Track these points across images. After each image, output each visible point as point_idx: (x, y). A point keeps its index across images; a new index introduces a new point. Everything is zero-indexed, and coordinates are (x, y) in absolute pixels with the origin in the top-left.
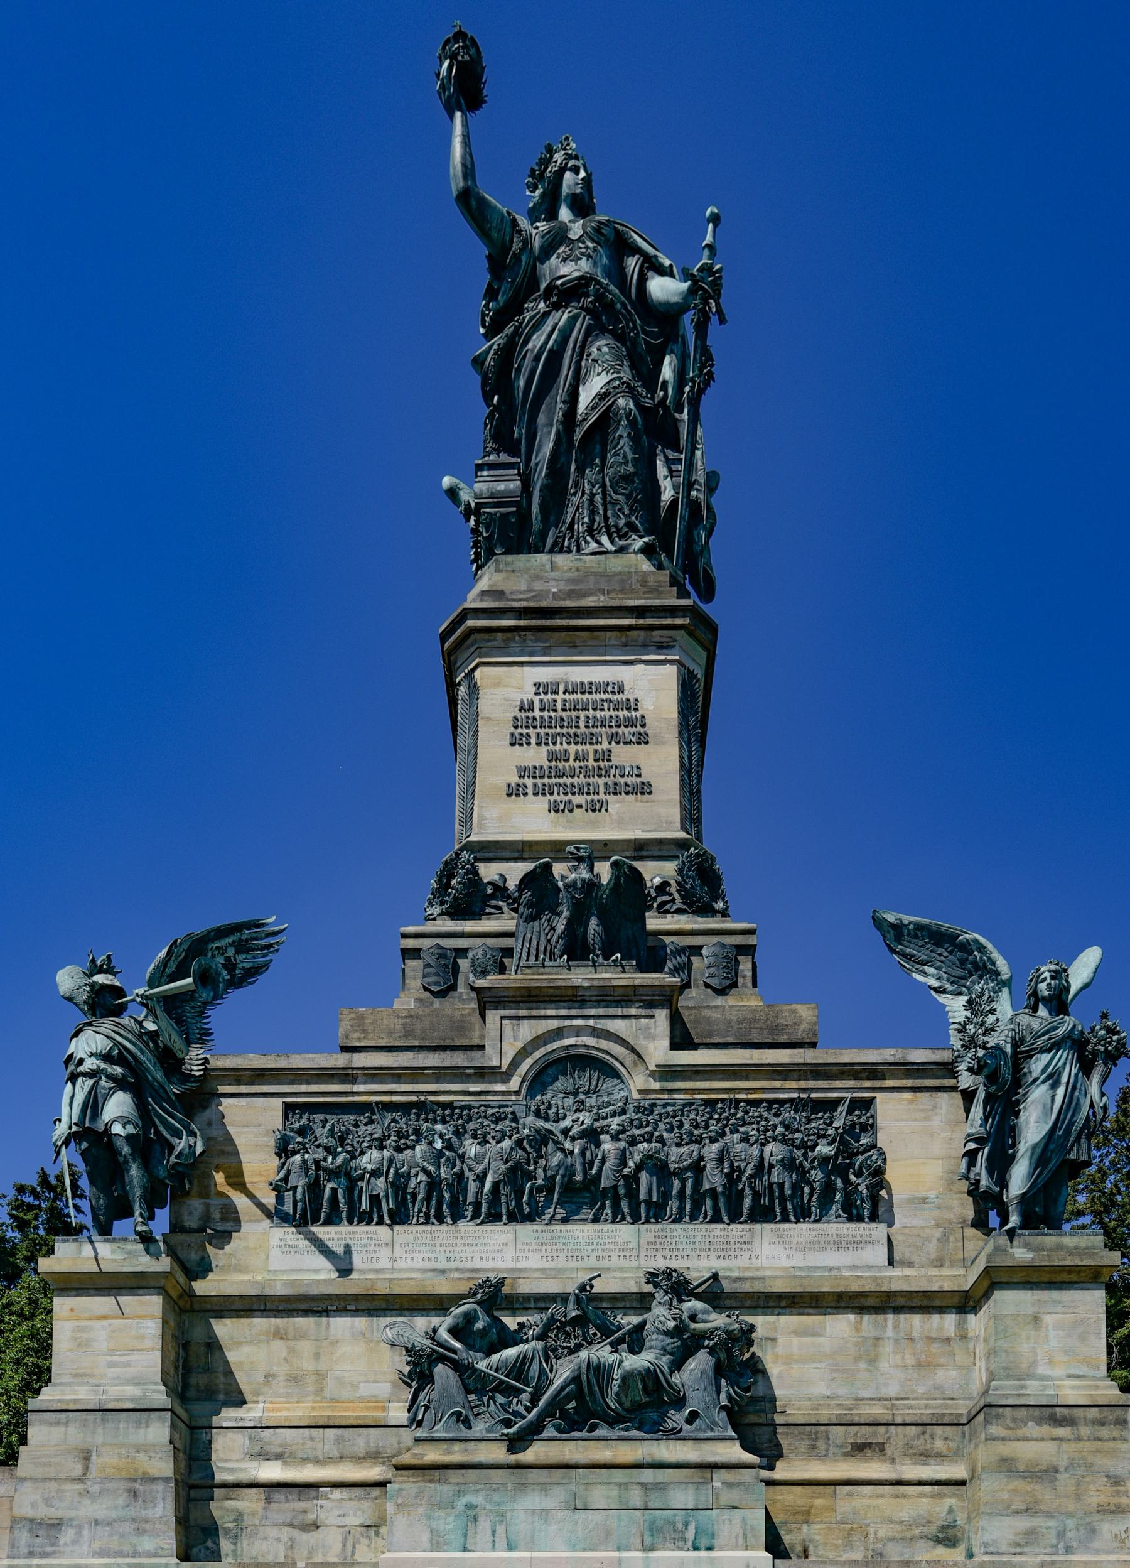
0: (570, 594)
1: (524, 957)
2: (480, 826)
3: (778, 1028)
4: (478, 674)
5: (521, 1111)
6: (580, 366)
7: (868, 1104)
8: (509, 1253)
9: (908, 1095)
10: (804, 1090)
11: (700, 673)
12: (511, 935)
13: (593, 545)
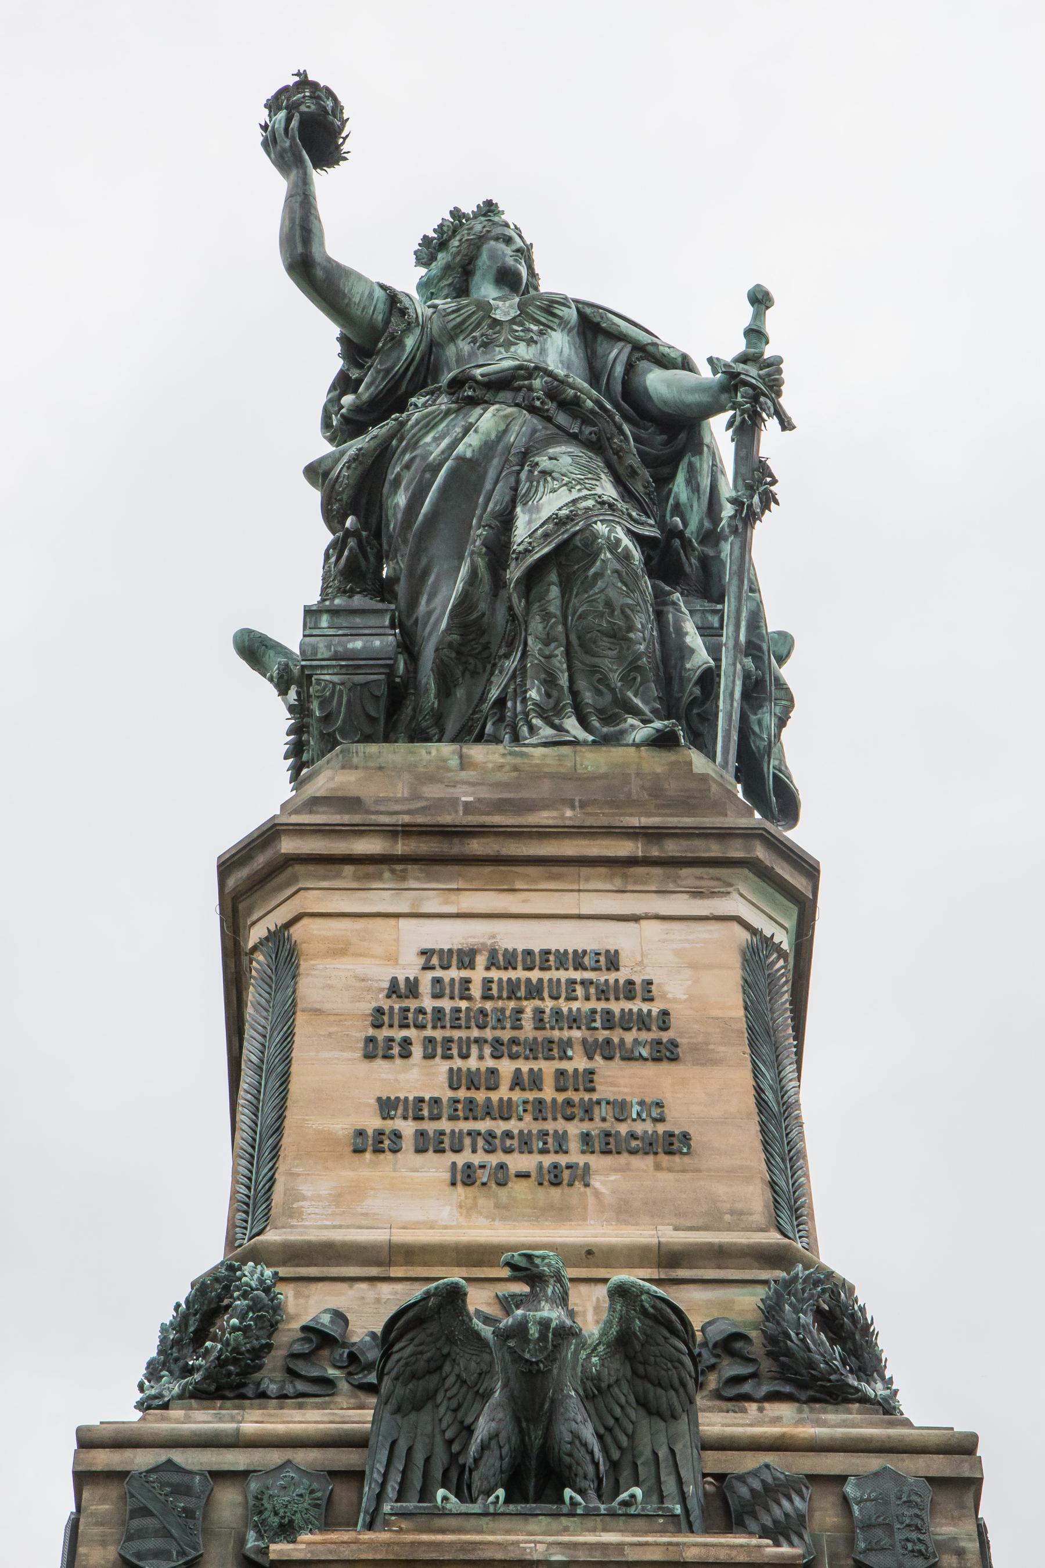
0: (501, 806)
1: (391, 1491)
2: (291, 1213)
4: (297, 932)
6: (518, 482)
11: (784, 940)
12: (358, 1442)
13: (547, 732)
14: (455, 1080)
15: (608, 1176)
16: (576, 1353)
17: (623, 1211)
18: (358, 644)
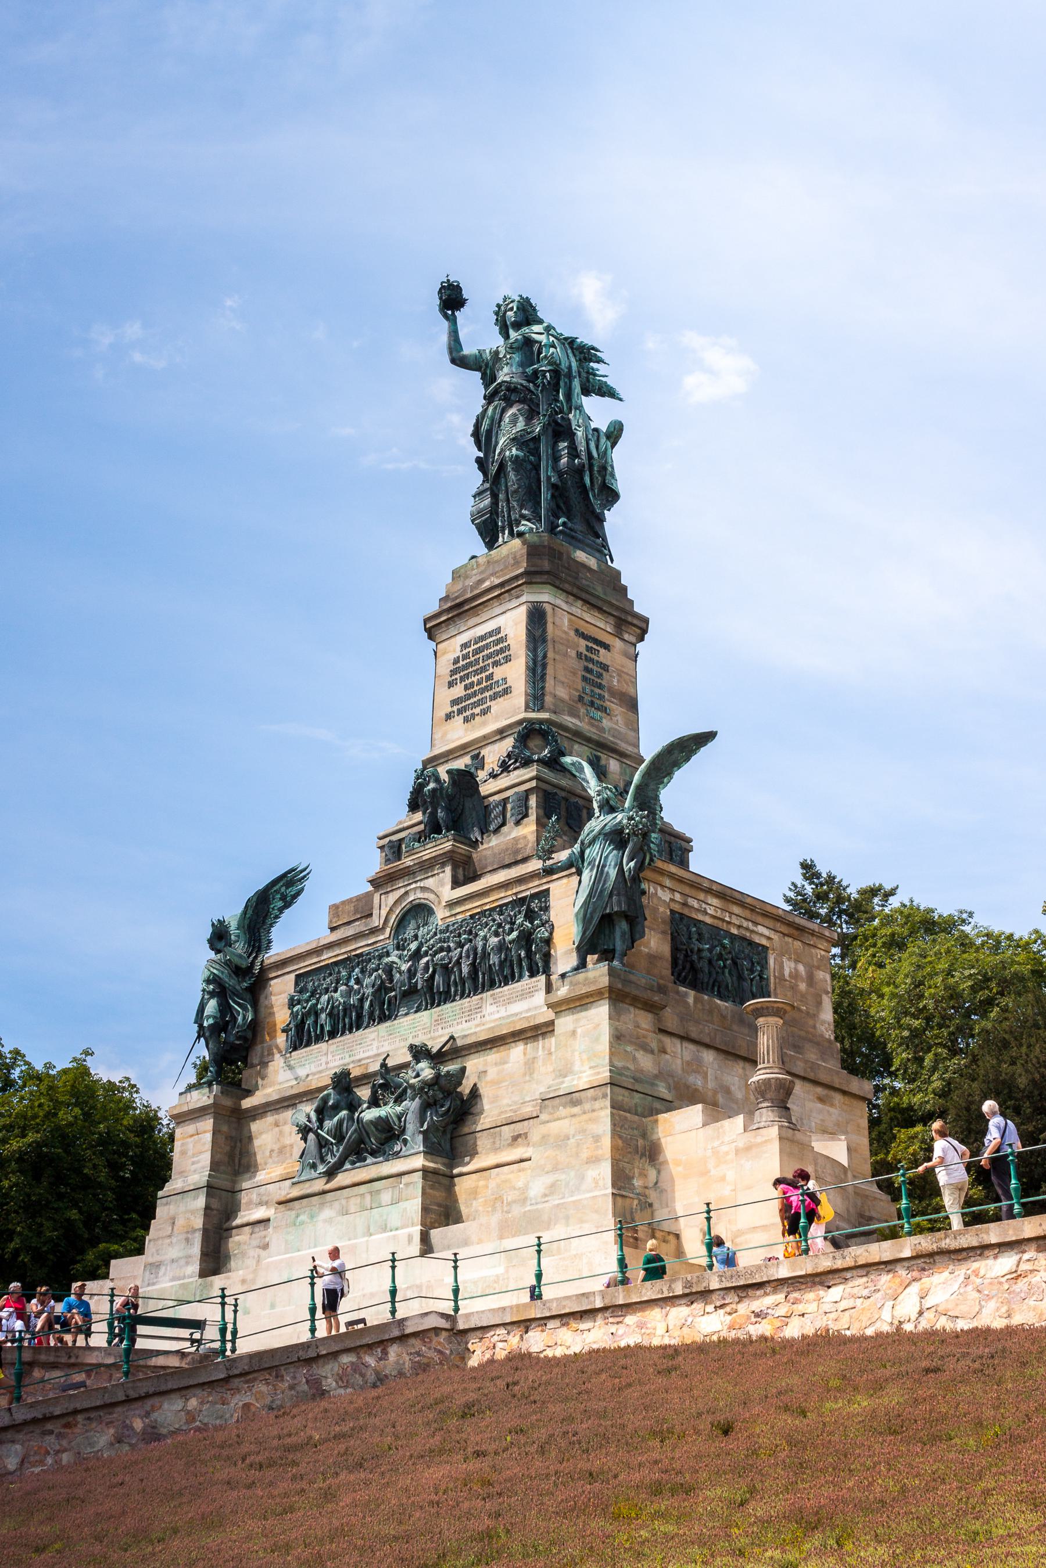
3: (517, 851)
5: (390, 948)
7: (548, 890)
8: (375, 1044)
9: (565, 880)
10: (516, 894)
14: (466, 688)
15: (496, 706)
16: (441, 793)
17: (497, 718)
18: (482, 505)
